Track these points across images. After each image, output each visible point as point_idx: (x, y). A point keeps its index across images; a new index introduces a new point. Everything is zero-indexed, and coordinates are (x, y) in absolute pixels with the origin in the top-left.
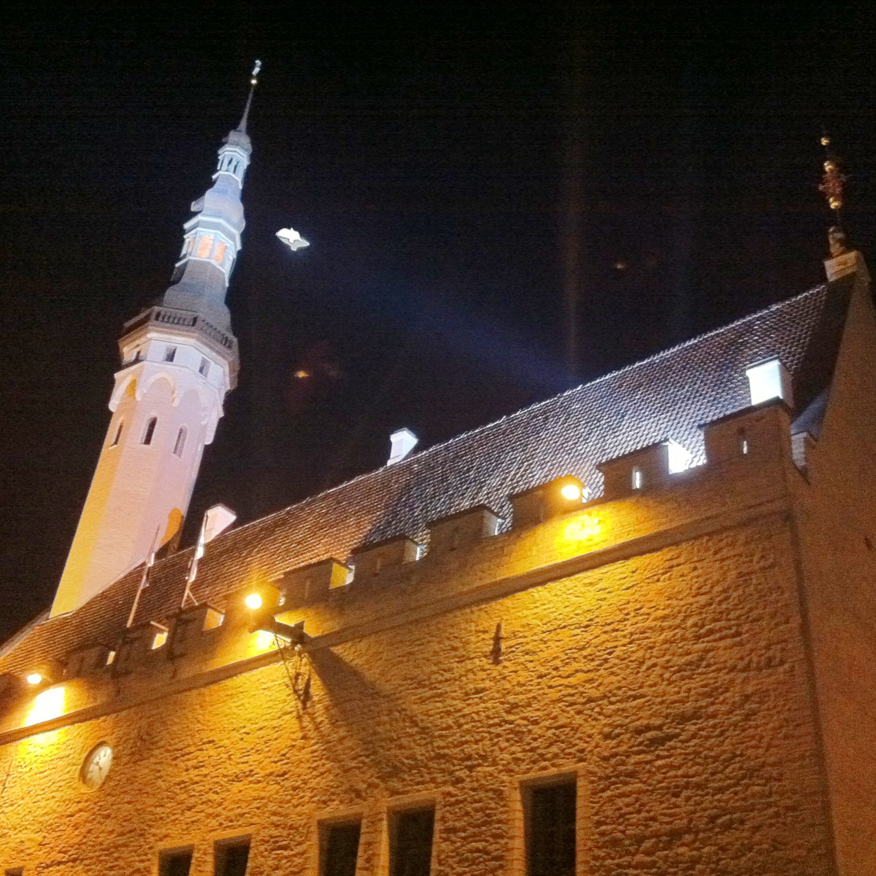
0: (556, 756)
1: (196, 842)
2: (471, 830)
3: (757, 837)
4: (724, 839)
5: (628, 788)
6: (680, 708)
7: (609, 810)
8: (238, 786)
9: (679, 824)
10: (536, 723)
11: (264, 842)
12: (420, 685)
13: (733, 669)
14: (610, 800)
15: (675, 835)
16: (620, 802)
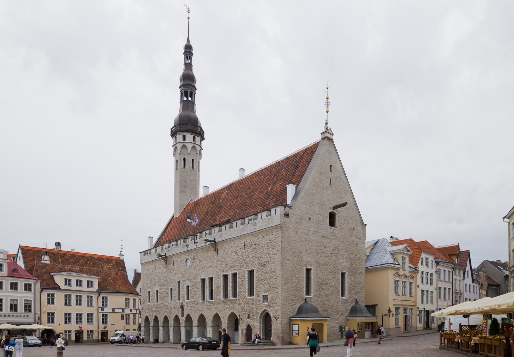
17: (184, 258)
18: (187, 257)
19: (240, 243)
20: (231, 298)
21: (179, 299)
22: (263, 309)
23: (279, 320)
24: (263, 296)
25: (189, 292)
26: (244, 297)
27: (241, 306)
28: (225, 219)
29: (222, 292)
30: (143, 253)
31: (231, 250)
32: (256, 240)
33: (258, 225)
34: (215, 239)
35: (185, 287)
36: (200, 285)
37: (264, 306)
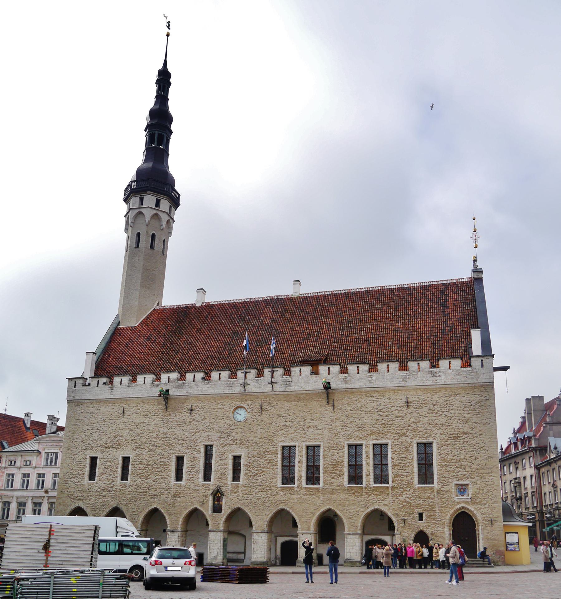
0: (427, 437)
1: (297, 444)
2: (401, 452)
3: (482, 462)
4: (473, 462)
5: (448, 448)
6: (462, 431)
7: (443, 452)
8: (310, 430)
9: (462, 457)
10: (421, 427)
11: (326, 447)
12: (380, 411)
13: (476, 423)
14: (444, 450)
15: (460, 459)
16: (446, 451)
17: (228, 405)
18: (237, 403)
19: (399, 399)
20: (372, 484)
21: (207, 477)
22: (459, 506)
23: (496, 524)
24: (456, 484)
25: (243, 468)
26: (410, 484)
27: (401, 498)
28: (313, 354)
29: (346, 473)
30: (81, 381)
31: (372, 405)
32: (435, 397)
33: (443, 377)
34: (329, 383)
35: (231, 458)
36: (280, 456)
37: (460, 502)
